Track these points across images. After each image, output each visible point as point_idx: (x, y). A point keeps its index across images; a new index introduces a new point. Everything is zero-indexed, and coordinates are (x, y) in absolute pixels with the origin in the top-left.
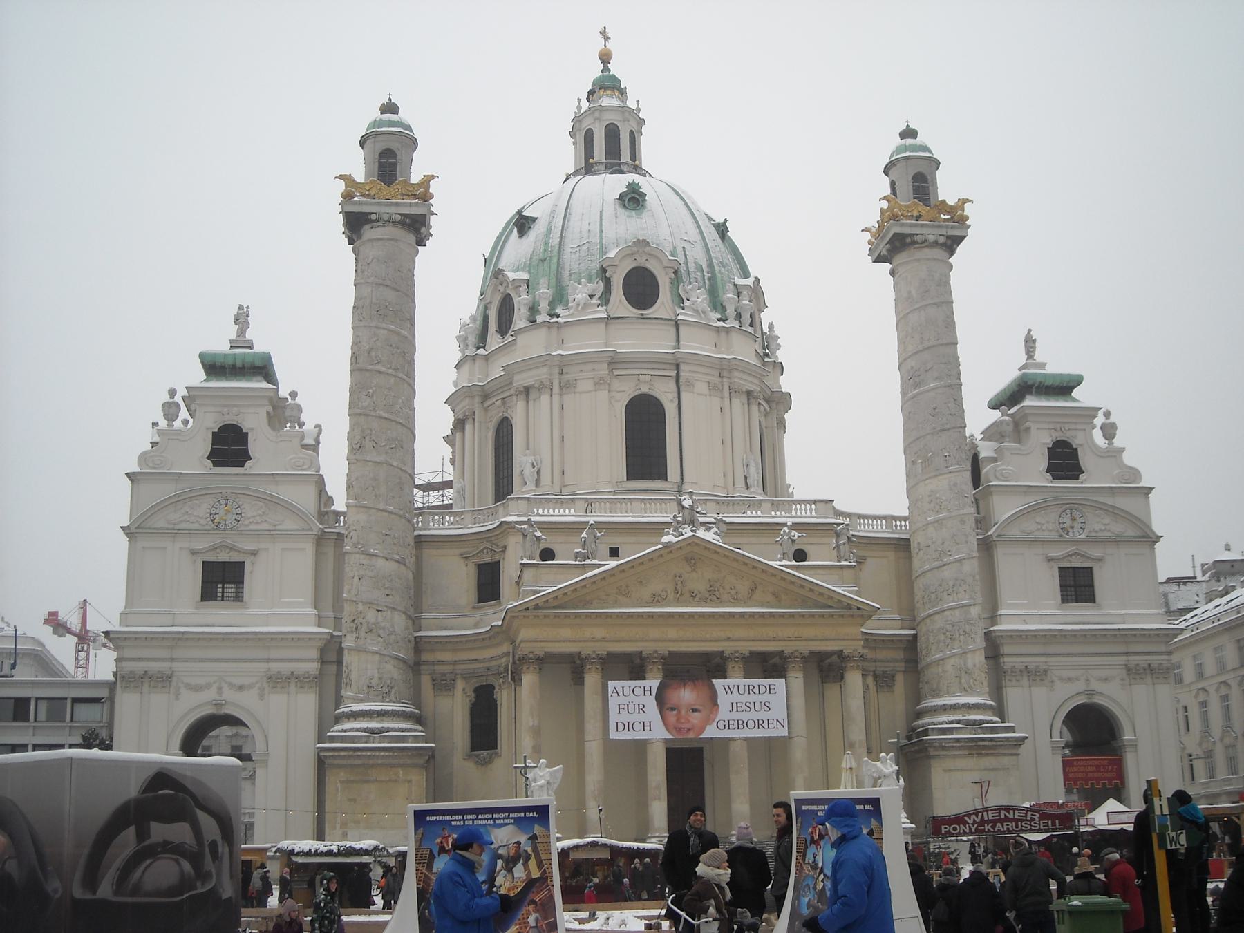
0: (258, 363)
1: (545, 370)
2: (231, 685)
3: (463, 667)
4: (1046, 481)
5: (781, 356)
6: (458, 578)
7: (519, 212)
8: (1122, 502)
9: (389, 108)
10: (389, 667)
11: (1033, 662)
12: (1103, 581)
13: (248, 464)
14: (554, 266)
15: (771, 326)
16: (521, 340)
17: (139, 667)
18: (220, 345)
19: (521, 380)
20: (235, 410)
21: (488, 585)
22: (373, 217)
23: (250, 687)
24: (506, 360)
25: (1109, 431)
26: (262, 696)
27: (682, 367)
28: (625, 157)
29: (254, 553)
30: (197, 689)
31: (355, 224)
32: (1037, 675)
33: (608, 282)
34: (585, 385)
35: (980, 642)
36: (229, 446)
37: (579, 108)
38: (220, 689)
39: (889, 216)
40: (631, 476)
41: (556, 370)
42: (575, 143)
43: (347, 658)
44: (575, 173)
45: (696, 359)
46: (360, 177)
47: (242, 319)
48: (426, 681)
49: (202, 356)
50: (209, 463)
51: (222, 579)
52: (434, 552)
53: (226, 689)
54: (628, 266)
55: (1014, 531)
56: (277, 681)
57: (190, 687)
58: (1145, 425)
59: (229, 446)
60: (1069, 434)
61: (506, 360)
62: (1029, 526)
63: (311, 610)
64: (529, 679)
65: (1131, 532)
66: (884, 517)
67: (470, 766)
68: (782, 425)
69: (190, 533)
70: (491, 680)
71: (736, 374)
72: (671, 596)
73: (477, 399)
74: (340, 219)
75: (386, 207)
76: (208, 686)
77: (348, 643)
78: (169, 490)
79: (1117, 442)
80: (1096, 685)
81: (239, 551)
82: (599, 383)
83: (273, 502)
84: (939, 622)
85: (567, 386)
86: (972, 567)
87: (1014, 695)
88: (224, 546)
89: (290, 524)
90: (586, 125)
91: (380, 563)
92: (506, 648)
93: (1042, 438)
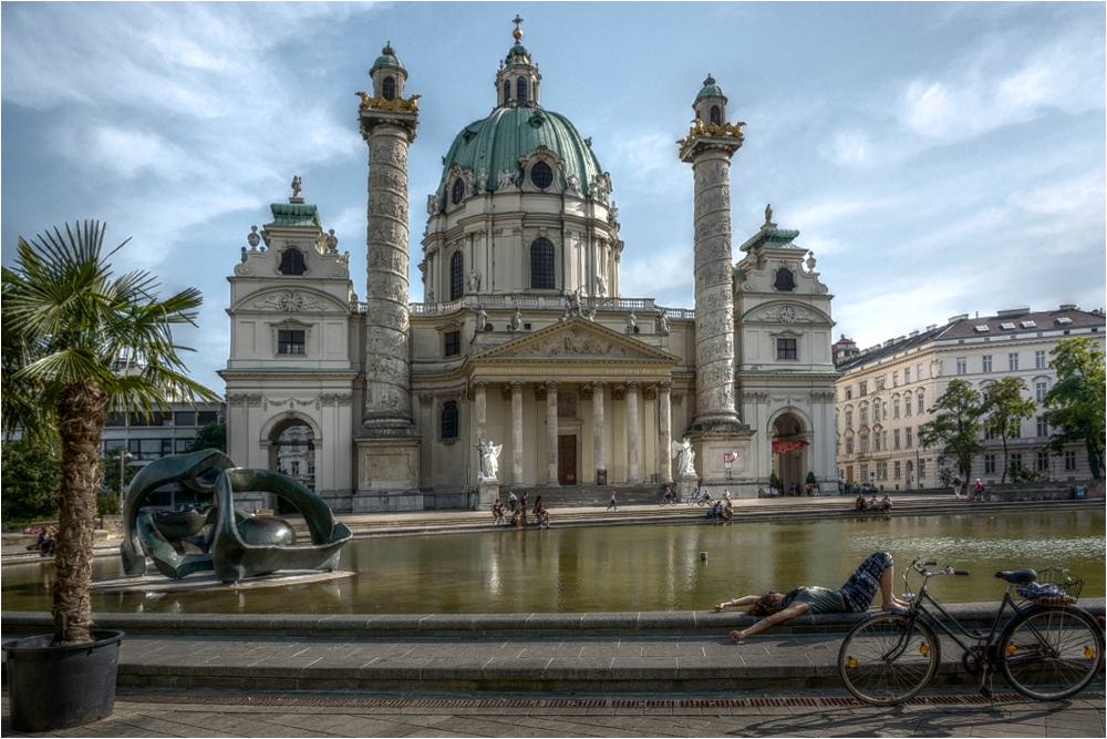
0: (309, 212)
1: (484, 223)
2: (298, 402)
3: (437, 391)
4: (769, 290)
5: (618, 220)
6: (433, 340)
7: (466, 128)
8: (817, 304)
9: (388, 51)
10: (395, 391)
13: (304, 273)
14: (489, 161)
15: (613, 203)
16: (469, 204)
18: (283, 196)
19: (468, 229)
20: (296, 240)
21: (453, 344)
22: (381, 121)
23: (311, 402)
24: (460, 217)
25: (812, 263)
26: (318, 408)
27: (566, 223)
29: (311, 325)
30: (277, 404)
32: (761, 397)
33: (522, 171)
34: (507, 232)
36: (293, 262)
37: (502, 67)
38: (292, 404)
40: (534, 286)
41: (490, 223)
42: (498, 90)
43: (369, 386)
44: (499, 107)
45: (573, 218)
46: (371, 94)
47: (296, 185)
48: (415, 398)
49: (272, 206)
50: (280, 273)
51: (291, 339)
52: (419, 326)
53: (295, 403)
54: (534, 160)
55: (755, 319)
56: (327, 400)
57: (272, 403)
59: (293, 262)
60: (789, 264)
61: (460, 217)
63: (346, 358)
64: (481, 397)
65: (818, 321)
66: (681, 310)
67: (442, 446)
68: (617, 259)
69: (270, 314)
70: (454, 398)
71: (597, 229)
72: (563, 351)
73: (441, 241)
74: (359, 123)
75: (386, 114)
76: (285, 402)
77: (370, 375)
78: (256, 286)
79: (815, 270)
81: (301, 324)
82: (516, 231)
83: (323, 295)
86: (730, 338)
88: (292, 321)
89: (332, 308)
90: (505, 77)
91: (389, 331)
92: (464, 380)
93: (772, 265)
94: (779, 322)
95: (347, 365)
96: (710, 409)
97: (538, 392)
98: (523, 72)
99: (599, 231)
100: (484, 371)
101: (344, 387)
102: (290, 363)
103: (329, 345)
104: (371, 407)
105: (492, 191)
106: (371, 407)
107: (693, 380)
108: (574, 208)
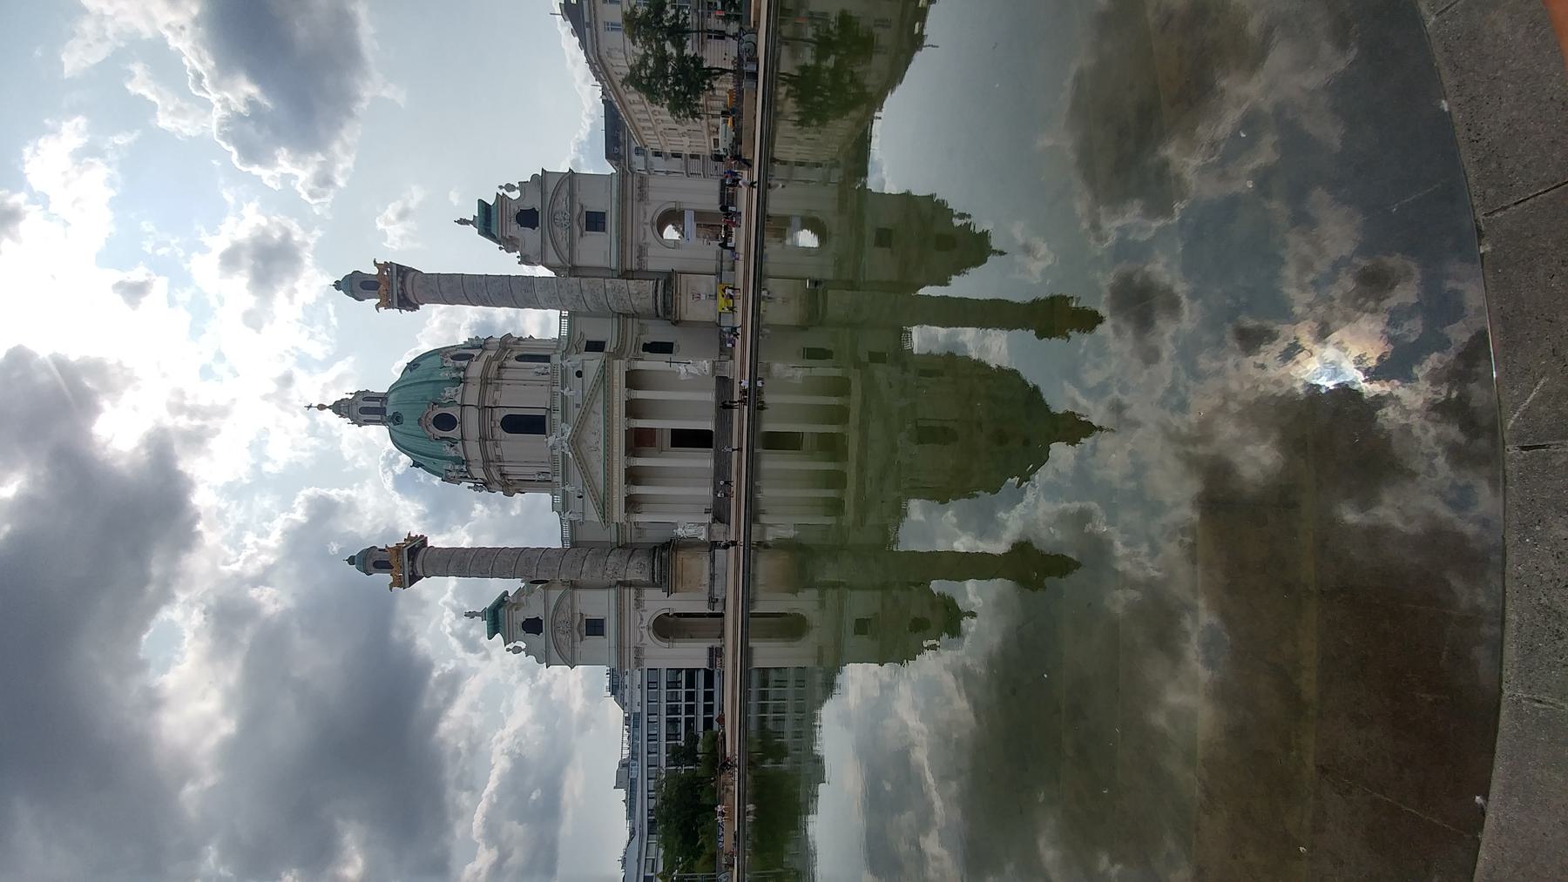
9: (351, 561)
11: (635, 254)
12: (596, 206)
17: (633, 661)
19: (497, 477)
25: (510, 187)
28: (377, 404)
31: (414, 579)
32: (642, 251)
34: (498, 451)
35: (622, 283)
39: (389, 306)
45: (482, 397)
51: (595, 627)
54: (432, 428)
58: (509, 167)
59: (533, 626)
62: (564, 245)
80: (648, 220)
83: (557, 608)
84: (614, 306)
85: (499, 459)
87: (652, 265)
94: (571, 228)
95: (612, 592)
96: (651, 306)
97: (633, 476)
98: (355, 410)
99: (492, 373)
100: (616, 514)
101: (630, 593)
102: (611, 627)
103: (597, 603)
104: (645, 578)
105: (465, 462)
106: (645, 578)
107: (626, 316)
108: (472, 395)
